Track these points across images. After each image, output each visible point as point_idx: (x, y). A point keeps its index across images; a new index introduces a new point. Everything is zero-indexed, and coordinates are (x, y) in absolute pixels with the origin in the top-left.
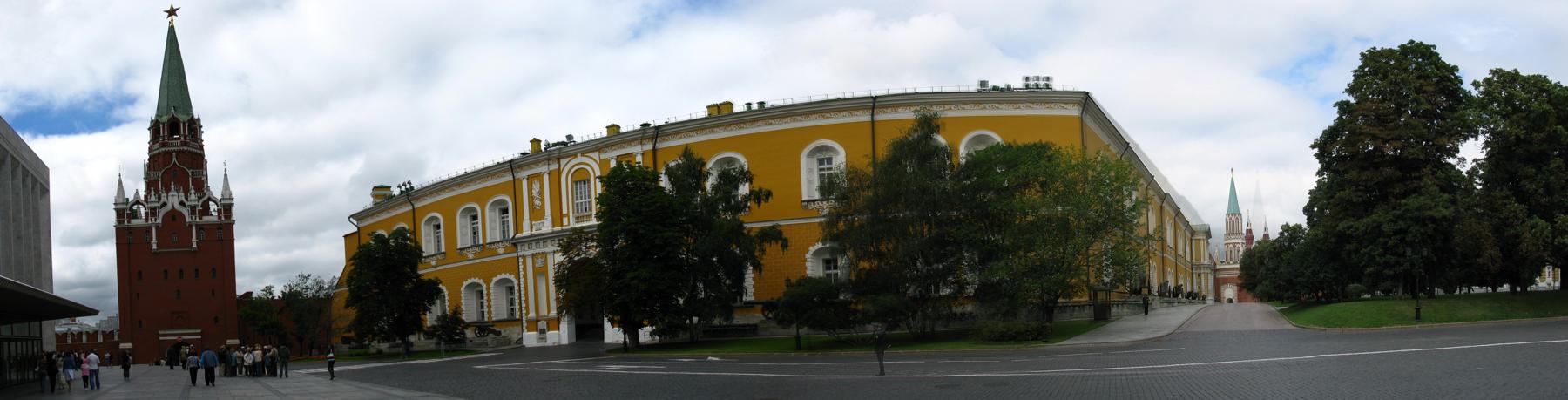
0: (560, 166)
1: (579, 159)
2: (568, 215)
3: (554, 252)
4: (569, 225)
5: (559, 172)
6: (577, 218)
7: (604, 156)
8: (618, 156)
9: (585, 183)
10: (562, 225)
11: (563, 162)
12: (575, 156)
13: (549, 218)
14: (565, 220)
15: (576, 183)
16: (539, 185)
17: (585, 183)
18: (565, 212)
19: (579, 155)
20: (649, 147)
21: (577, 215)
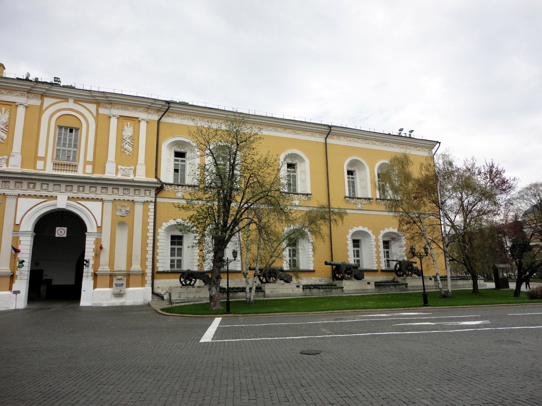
0: (42, 103)
1: (70, 104)
2: (44, 159)
3: (19, 196)
4: (44, 169)
5: (41, 110)
6: (55, 164)
7: (102, 111)
8: (120, 116)
9: (71, 131)
10: (35, 168)
11: (48, 101)
12: (66, 100)
13: (19, 157)
14: (40, 164)
15: (60, 127)
16: (7, 116)
17: (71, 131)
18: (41, 153)
19: (71, 101)
20: (155, 117)
21: (57, 161)
